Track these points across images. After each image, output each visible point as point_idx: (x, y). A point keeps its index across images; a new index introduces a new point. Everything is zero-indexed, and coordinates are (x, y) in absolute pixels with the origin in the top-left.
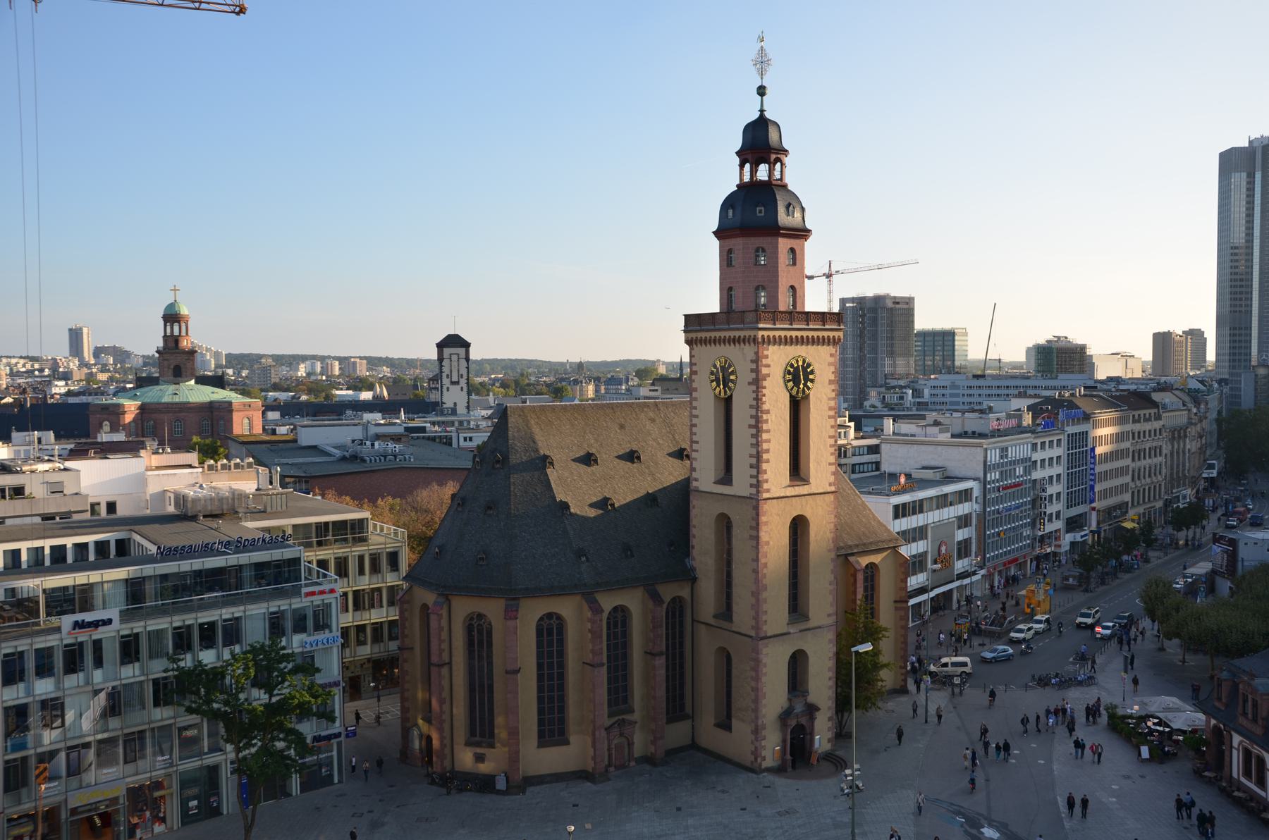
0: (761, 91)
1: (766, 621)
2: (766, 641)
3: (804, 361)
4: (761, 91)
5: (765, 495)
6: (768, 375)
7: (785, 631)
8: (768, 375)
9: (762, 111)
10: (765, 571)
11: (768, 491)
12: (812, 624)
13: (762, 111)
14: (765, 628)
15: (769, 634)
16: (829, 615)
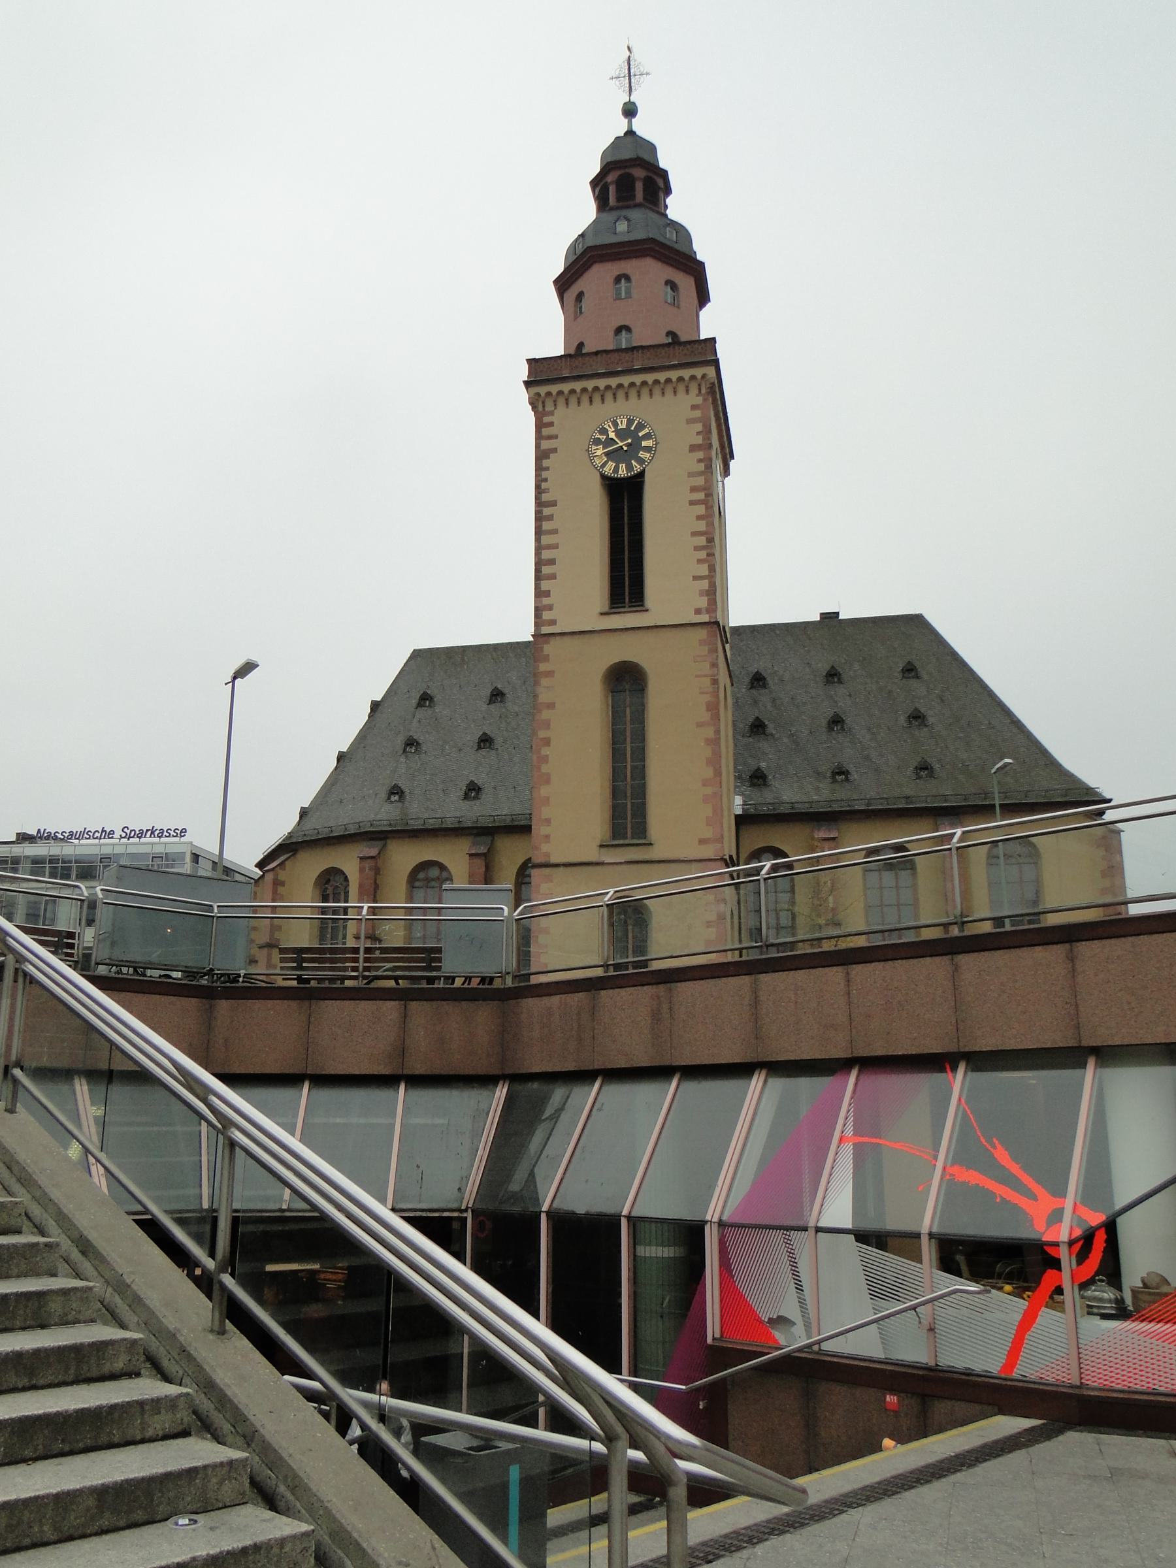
0: (630, 111)
1: (547, 837)
2: (547, 871)
3: (630, 422)
4: (630, 111)
5: (545, 630)
6: (555, 450)
7: (593, 855)
8: (555, 450)
9: (630, 133)
10: (545, 751)
11: (553, 622)
12: (655, 853)
13: (630, 133)
14: (545, 848)
15: (553, 860)
16: (702, 842)
